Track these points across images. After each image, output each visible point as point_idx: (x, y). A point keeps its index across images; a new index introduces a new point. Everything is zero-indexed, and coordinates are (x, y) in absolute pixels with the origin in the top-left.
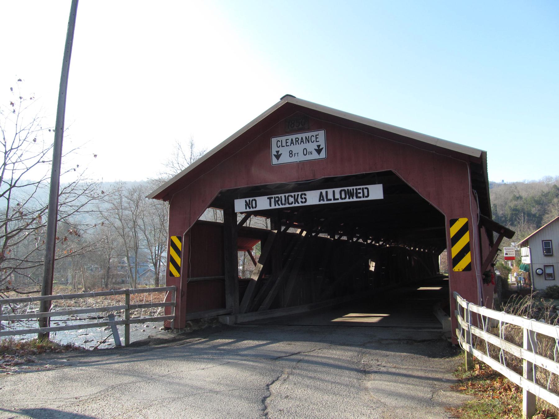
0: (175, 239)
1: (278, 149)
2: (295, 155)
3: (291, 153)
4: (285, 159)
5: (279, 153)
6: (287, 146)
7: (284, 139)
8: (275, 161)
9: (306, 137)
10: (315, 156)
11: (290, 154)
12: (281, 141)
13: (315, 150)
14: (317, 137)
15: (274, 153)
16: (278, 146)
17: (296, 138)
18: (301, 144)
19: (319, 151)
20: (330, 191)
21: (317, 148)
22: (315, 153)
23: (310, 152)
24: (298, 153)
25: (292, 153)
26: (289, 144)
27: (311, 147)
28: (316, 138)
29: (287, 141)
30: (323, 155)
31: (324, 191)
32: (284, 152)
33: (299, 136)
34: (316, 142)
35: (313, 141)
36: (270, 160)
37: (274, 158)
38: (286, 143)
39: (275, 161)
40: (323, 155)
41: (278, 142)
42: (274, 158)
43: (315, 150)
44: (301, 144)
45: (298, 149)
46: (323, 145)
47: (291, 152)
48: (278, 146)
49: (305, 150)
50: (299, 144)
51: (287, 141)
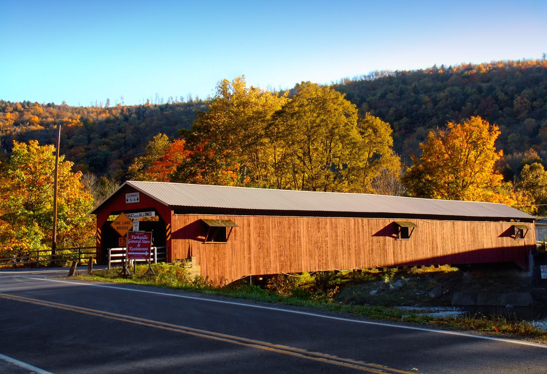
0: (99, 229)
3: (131, 200)
4: (129, 202)
7: (129, 194)
8: (127, 202)
10: (137, 201)
15: (126, 199)
19: (138, 199)
20: (142, 213)
22: (137, 200)
27: (136, 198)
30: (139, 201)
31: (141, 213)
32: (129, 199)
33: (133, 194)
36: (125, 202)
37: (126, 201)
39: (127, 202)
40: (139, 201)
42: (126, 201)
45: (132, 198)
46: (139, 198)
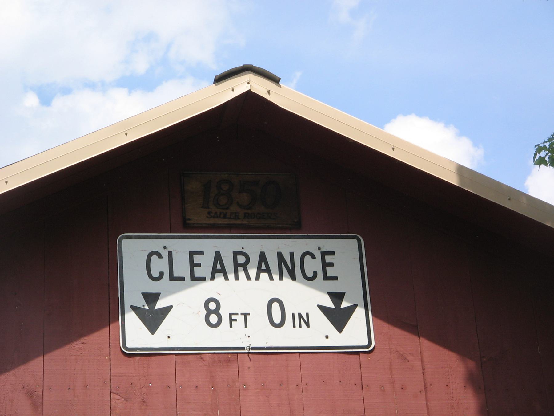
1: (152, 287)
2: (231, 320)
5: (160, 304)
6: (194, 278)
9: (280, 255)
11: (209, 312)
12: (165, 254)
13: (323, 309)
14: (328, 259)
16: (155, 274)
17: (236, 254)
18: (257, 278)
21: (329, 303)
23: (300, 316)
24: (245, 315)
25: (216, 311)
26: (204, 270)
28: (325, 265)
29: (197, 259)
34: (326, 278)
35: (310, 274)
38: (193, 265)
41: (154, 258)
43: (323, 309)
44: (257, 278)
47: (212, 306)
48: (155, 274)
49: (275, 306)
50: (249, 278)
51: (197, 259)
